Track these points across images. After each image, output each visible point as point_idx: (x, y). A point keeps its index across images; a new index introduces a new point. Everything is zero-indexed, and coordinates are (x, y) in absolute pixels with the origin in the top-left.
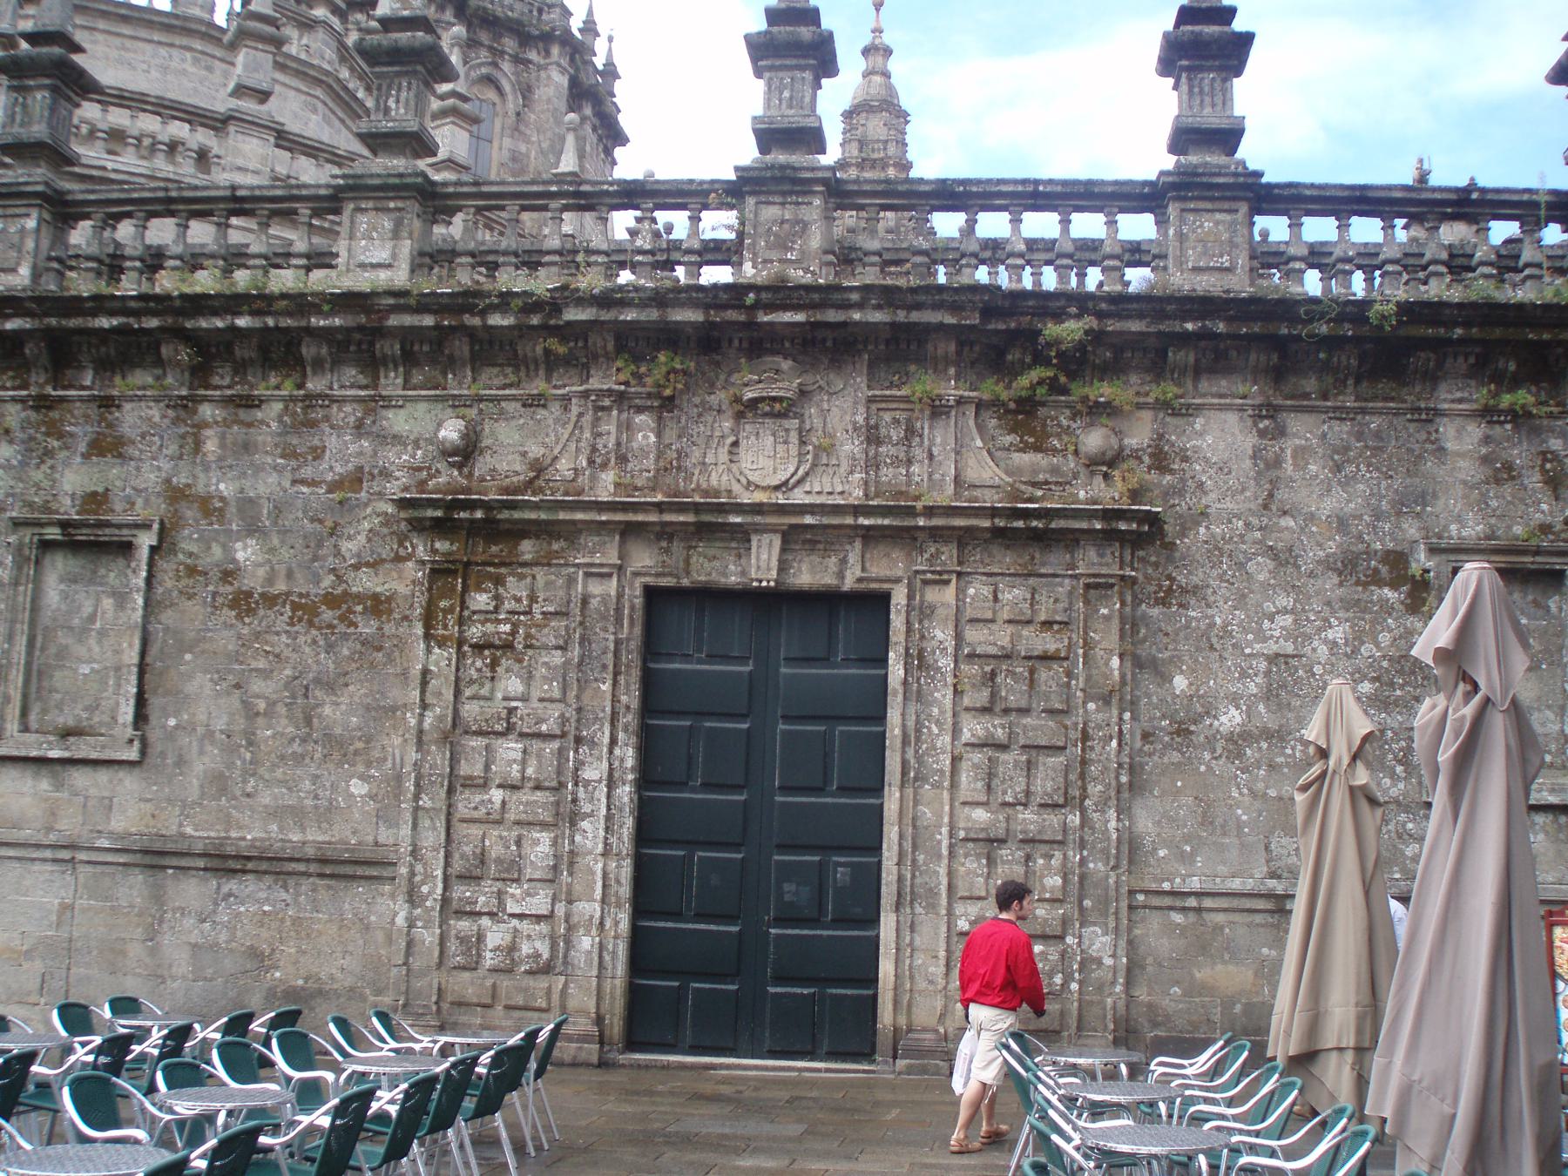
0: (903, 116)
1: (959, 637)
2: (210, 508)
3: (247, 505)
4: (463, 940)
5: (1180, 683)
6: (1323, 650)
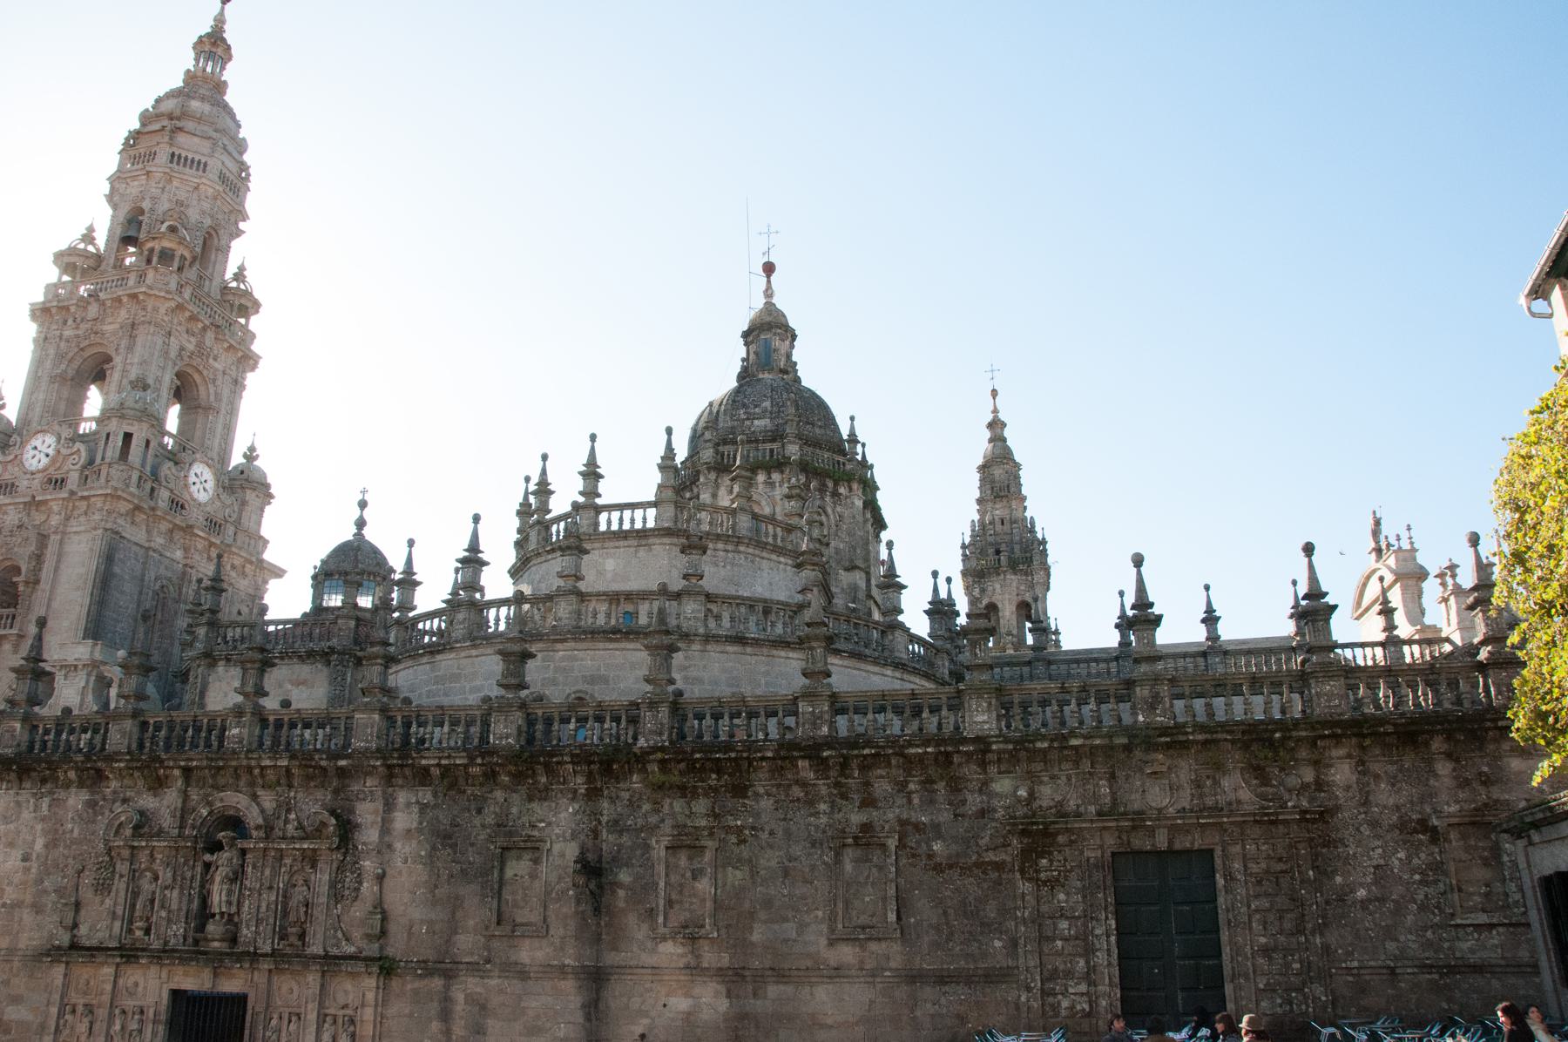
0: (1017, 466)
1: (1245, 866)
2: (918, 827)
3: (936, 827)
4: (1052, 1005)
5: (1339, 879)
6: (1397, 862)
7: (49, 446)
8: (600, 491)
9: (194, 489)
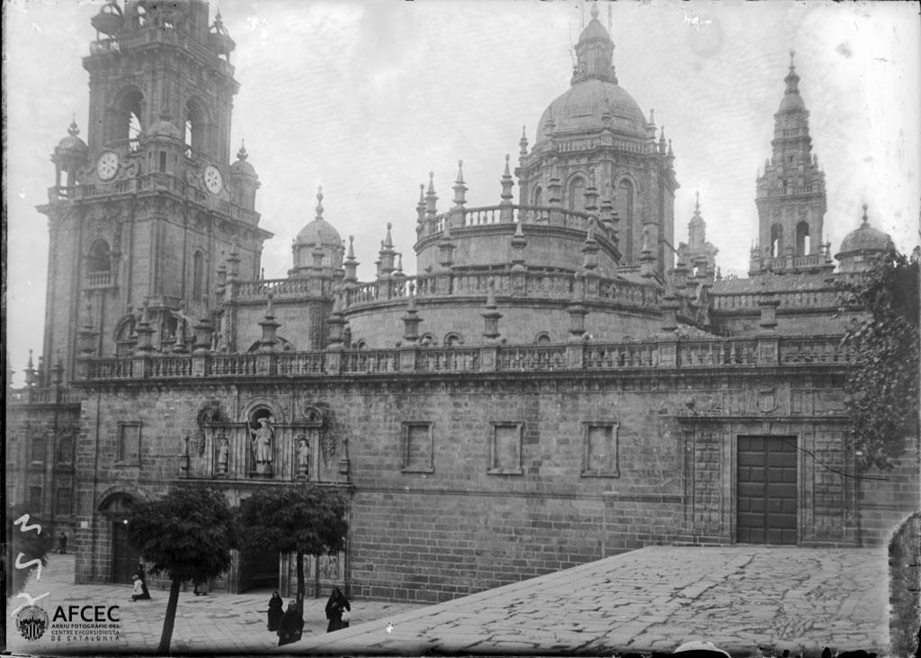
7: (113, 161)
8: (466, 199)
9: (209, 184)
